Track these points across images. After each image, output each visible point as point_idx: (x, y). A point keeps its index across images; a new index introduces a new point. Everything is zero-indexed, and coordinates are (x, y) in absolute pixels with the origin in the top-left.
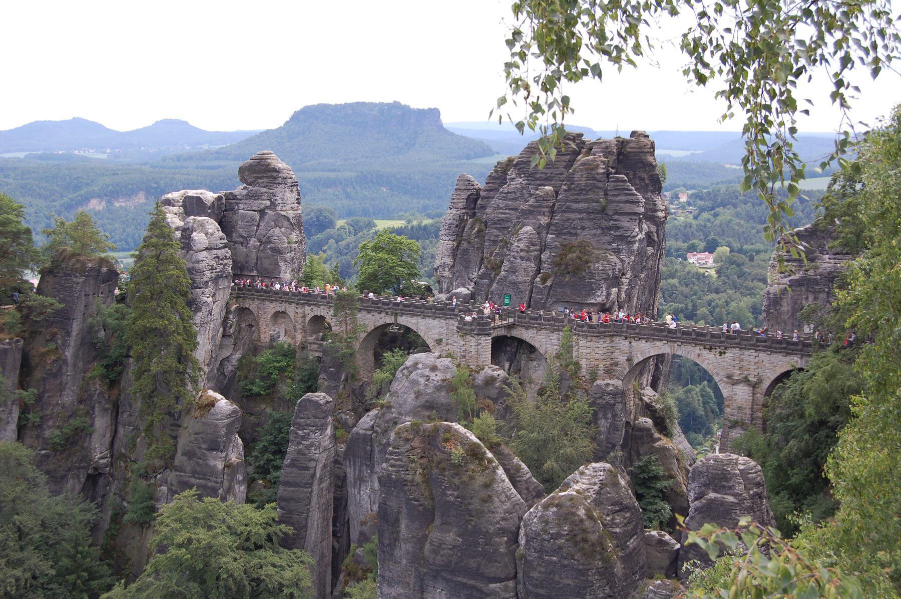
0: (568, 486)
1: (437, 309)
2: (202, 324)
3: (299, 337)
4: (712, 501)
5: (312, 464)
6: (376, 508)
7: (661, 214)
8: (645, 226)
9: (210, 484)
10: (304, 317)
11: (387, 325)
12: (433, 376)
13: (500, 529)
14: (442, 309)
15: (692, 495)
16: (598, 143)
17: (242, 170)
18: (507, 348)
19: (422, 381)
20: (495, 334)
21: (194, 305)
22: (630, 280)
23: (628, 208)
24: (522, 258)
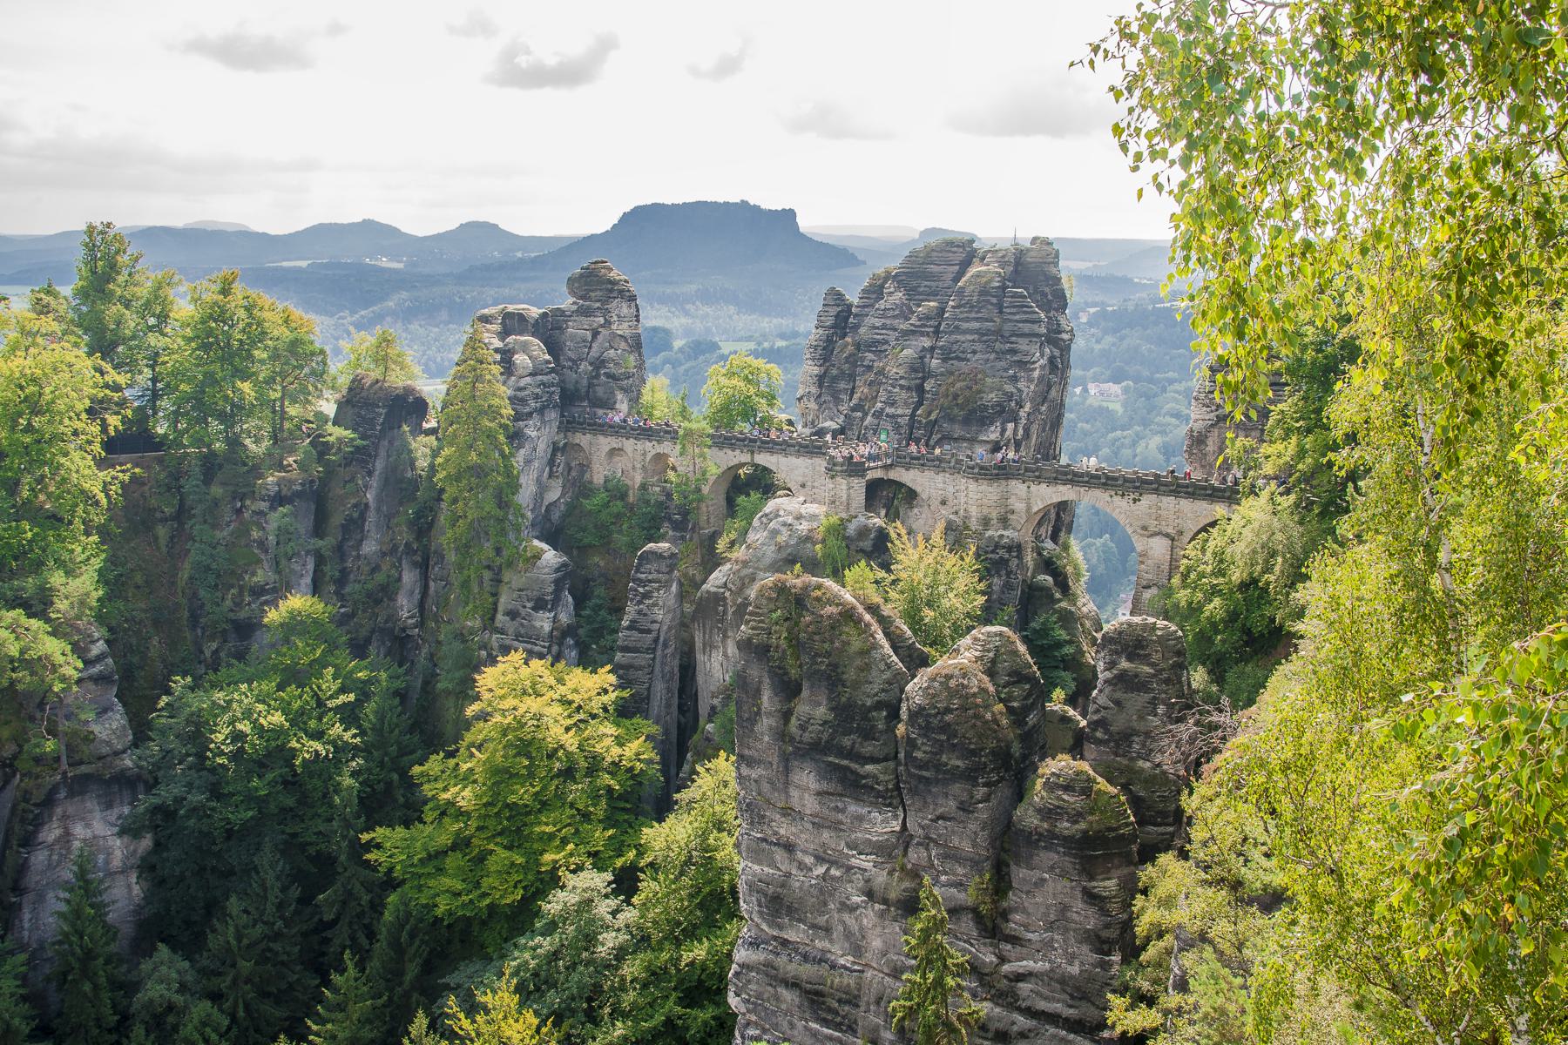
1: (801, 445)
2: (528, 462)
3: (638, 479)
5: (656, 626)
7: (1065, 336)
8: (1047, 350)
9: (537, 649)
10: (644, 454)
13: (879, 702)
14: (806, 447)
19: (784, 529)
20: (870, 475)
23: (1027, 328)
24: (902, 387)
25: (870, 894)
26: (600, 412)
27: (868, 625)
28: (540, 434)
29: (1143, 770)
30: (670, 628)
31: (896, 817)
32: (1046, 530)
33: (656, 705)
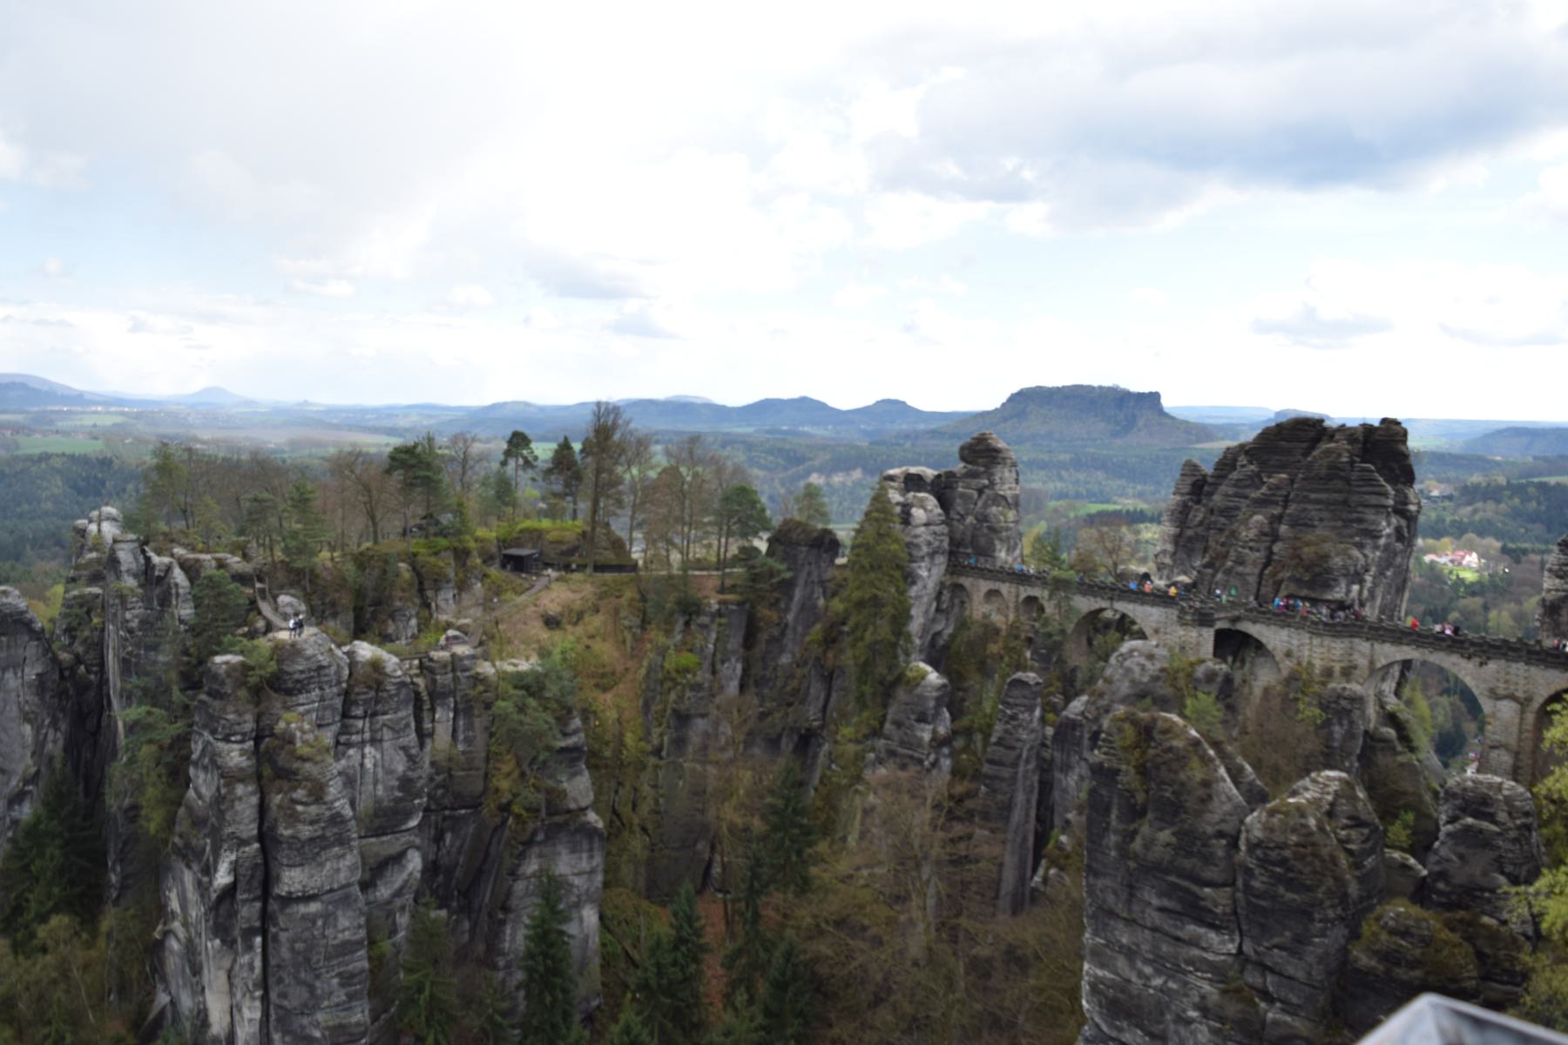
0: (1294, 793)
2: (918, 597)
4: (1468, 828)
5: (1019, 745)
6: (1083, 795)
7: (1413, 508)
10: (1017, 596)
11: (1102, 610)
12: (1148, 665)
15: (1444, 817)
16: (1342, 428)
17: (962, 449)
18: (1232, 644)
19: (1137, 670)
20: (1220, 625)
21: (910, 578)
22: (1374, 577)
25: (1204, 1010)
26: (982, 559)
27: (1211, 760)
28: (929, 574)
29: (1484, 926)
30: (1032, 748)
31: (1232, 941)
32: (1389, 686)
33: (1017, 816)
